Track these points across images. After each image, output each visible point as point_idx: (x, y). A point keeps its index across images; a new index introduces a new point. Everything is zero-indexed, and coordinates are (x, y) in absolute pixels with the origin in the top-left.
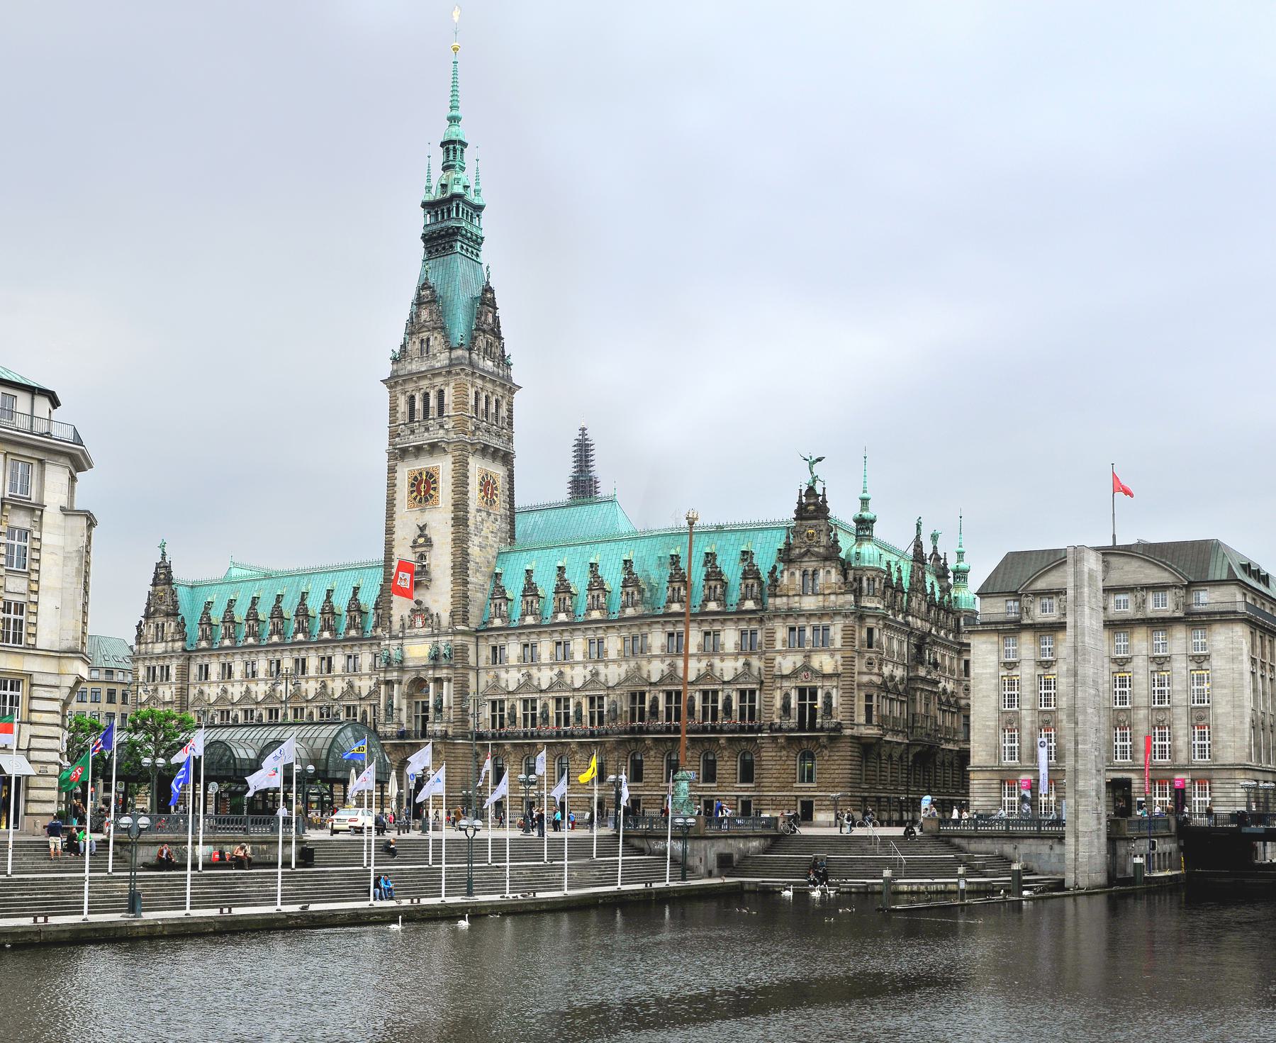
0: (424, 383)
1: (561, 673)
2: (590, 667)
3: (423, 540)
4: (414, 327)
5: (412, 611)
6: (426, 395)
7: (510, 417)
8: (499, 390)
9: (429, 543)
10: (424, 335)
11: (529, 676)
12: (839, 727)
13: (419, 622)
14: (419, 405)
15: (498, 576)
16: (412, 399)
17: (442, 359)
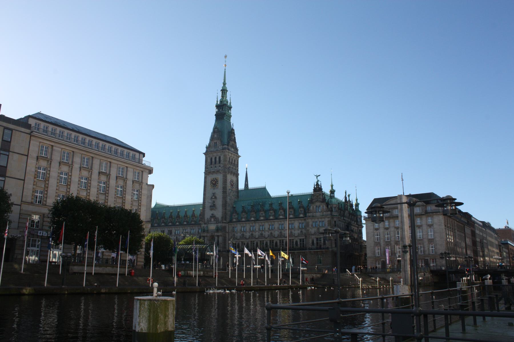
0: (215, 154)
1: (252, 234)
2: (260, 232)
3: (214, 196)
4: (212, 138)
5: (211, 217)
6: (216, 158)
7: (238, 164)
8: (235, 157)
9: (216, 198)
10: (216, 141)
11: (243, 235)
12: (328, 248)
13: (212, 220)
14: (213, 160)
15: (234, 207)
16: (211, 159)
17: (220, 147)
